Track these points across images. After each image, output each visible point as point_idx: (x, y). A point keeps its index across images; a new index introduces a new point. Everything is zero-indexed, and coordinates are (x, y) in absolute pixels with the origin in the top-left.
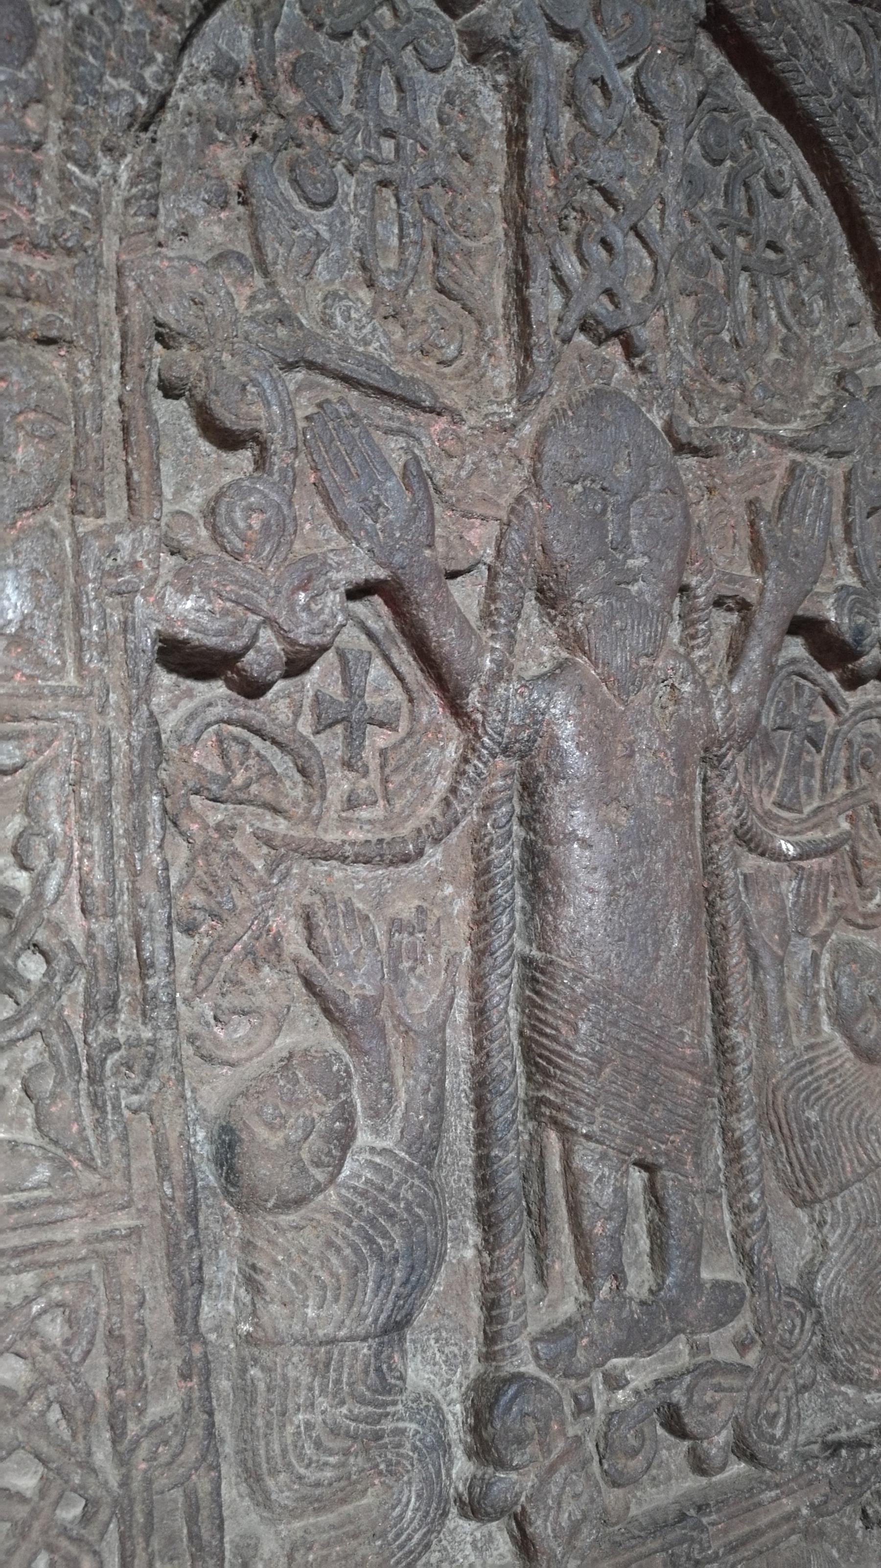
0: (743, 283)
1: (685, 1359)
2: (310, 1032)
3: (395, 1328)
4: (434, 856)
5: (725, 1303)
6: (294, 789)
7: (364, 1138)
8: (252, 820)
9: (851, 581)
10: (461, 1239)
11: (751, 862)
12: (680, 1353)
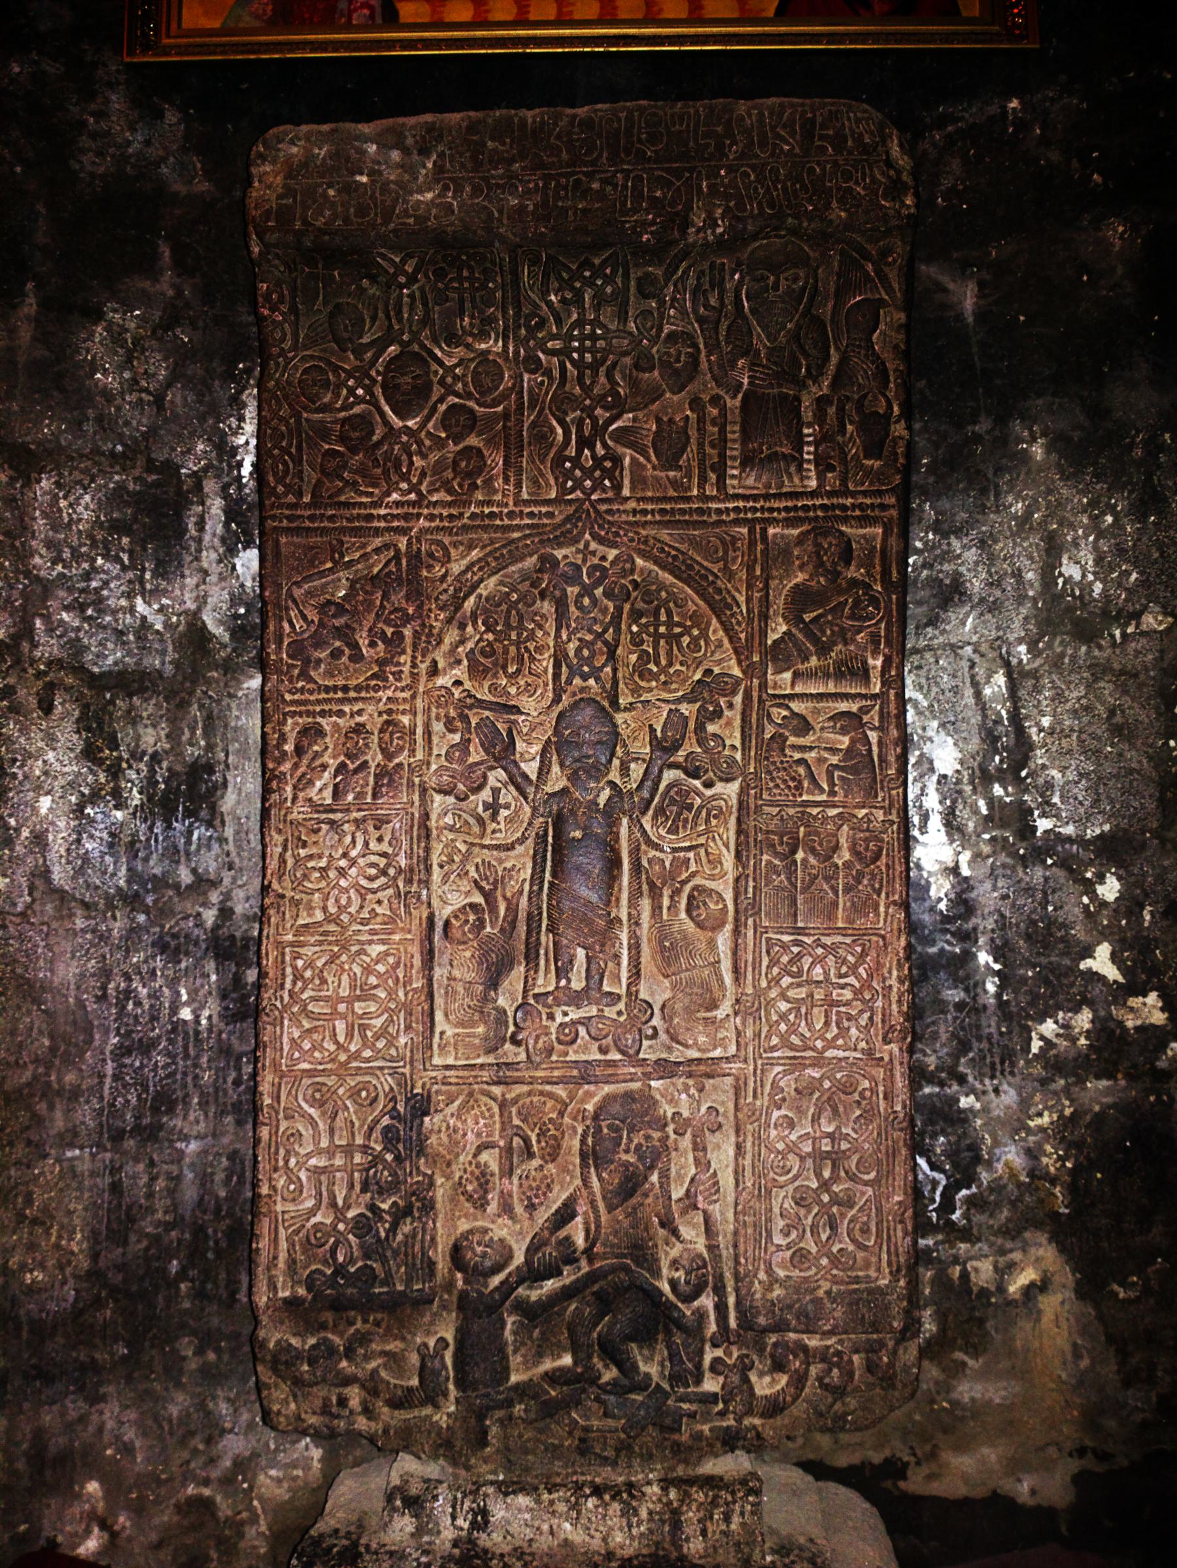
0: (662, 642)
1: (594, 1012)
2: (478, 899)
3: (493, 983)
4: (520, 849)
5: (614, 998)
6: (476, 829)
7: (488, 929)
8: (462, 837)
10: (520, 963)
11: (652, 853)
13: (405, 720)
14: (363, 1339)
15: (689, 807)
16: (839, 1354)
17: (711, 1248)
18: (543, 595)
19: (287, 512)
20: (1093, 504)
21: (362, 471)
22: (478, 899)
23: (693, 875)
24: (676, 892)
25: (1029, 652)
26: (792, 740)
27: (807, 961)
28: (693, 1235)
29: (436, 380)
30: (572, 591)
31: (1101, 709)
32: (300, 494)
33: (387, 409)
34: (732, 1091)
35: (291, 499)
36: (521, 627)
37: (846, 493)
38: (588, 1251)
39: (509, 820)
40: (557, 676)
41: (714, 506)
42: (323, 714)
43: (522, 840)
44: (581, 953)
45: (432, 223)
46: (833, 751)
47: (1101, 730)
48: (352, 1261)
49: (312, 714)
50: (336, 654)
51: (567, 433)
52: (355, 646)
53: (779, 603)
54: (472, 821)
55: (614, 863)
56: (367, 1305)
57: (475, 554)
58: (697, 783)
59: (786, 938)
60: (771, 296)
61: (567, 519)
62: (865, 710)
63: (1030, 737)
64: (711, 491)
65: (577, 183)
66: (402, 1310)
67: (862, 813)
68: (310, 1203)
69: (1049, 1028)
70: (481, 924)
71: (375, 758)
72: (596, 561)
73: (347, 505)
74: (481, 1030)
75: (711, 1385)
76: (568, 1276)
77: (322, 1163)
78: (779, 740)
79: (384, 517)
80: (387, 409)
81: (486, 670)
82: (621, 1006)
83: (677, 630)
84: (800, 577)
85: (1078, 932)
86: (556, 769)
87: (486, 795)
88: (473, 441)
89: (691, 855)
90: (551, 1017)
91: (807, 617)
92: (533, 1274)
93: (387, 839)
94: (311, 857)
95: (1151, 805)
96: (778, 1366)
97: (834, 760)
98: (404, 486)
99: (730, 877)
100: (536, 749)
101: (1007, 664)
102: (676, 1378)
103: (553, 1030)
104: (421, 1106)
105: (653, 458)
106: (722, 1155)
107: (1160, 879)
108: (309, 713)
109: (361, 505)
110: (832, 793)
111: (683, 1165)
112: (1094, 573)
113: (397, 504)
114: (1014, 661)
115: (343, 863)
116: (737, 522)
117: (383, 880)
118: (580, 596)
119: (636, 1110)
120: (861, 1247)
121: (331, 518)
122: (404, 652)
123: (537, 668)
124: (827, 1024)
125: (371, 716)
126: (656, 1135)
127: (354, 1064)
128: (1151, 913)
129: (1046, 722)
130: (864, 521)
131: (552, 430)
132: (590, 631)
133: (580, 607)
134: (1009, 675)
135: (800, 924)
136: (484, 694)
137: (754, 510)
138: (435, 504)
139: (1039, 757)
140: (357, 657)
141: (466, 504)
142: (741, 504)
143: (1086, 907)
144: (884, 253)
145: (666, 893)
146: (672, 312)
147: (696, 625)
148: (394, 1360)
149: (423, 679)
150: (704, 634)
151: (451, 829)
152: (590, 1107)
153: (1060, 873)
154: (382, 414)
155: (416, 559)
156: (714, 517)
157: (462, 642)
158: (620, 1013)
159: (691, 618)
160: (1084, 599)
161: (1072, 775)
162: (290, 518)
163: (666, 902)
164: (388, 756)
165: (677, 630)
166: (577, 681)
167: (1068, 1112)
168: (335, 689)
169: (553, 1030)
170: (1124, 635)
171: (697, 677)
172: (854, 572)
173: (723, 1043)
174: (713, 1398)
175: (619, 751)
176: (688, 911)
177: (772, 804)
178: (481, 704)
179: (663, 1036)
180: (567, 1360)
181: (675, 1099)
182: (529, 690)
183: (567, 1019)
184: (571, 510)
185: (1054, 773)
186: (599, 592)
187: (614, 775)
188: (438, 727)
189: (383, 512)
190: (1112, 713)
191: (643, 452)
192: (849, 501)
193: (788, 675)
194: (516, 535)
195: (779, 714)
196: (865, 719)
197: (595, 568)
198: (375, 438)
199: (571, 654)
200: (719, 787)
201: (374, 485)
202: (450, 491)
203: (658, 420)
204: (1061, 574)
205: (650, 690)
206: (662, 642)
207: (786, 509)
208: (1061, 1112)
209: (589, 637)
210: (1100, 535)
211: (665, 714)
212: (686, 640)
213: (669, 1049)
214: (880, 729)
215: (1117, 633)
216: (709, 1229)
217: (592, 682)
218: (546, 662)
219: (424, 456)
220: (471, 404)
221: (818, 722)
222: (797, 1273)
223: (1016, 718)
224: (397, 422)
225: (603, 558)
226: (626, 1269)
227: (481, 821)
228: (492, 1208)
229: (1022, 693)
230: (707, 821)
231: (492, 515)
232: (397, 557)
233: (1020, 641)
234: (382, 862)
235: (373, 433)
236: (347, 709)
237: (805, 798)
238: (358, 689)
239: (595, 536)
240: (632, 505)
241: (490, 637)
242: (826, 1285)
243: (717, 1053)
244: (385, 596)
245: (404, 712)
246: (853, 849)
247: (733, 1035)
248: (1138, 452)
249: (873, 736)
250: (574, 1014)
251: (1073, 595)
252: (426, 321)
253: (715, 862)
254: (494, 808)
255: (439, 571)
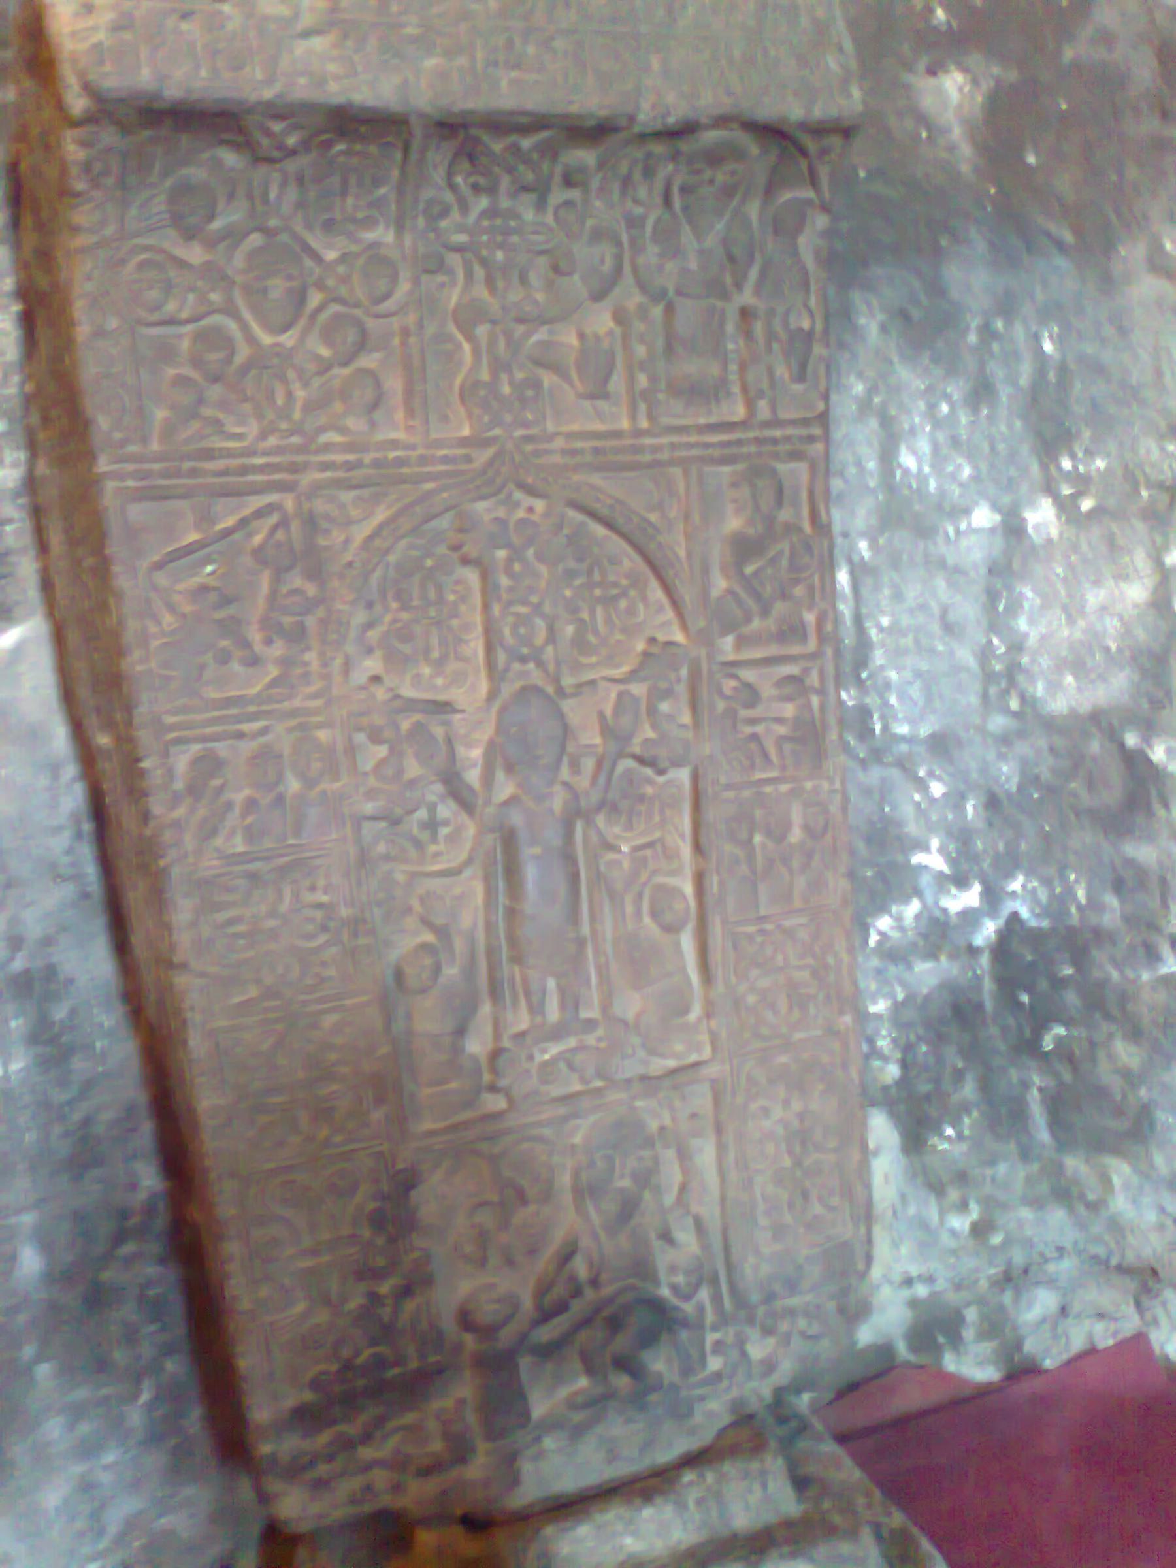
3: (460, 1032)
4: (467, 873)
5: (591, 1024)
6: (413, 853)
9: (651, 734)
11: (611, 856)
12: (572, 1042)
13: (323, 735)
14: (381, 1420)
15: (642, 798)
16: (818, 1307)
17: (705, 1247)
18: (466, 561)
19: (130, 467)
20: (930, 389)
21: (223, 405)
22: (428, 937)
23: (655, 872)
24: (640, 896)
25: (871, 547)
26: (744, 713)
27: (769, 951)
28: (686, 1237)
29: (311, 280)
30: (501, 554)
31: (936, 609)
32: (144, 440)
33: (247, 315)
34: (709, 1096)
35: (132, 448)
36: (441, 600)
37: (775, 423)
38: (594, 1282)
39: (452, 839)
40: (490, 664)
41: (648, 441)
42: (216, 738)
43: (470, 861)
44: (551, 984)
45: (333, 87)
46: (779, 720)
47: (936, 627)
48: (357, 1354)
49: (204, 739)
50: (224, 659)
51: (476, 352)
52: (246, 644)
53: (717, 553)
54: (408, 846)
55: (575, 877)
56: (378, 1390)
57: (381, 515)
58: (649, 771)
59: (751, 929)
60: (706, 191)
61: (490, 463)
62: (806, 671)
63: (869, 637)
64: (644, 424)
65: (510, 44)
66: (418, 1385)
67: (808, 785)
68: (300, 1307)
69: (884, 923)
70: (437, 969)
71: (293, 785)
72: (521, 514)
73: (209, 454)
74: (454, 1085)
75: (714, 1364)
76: (577, 1308)
77: (308, 1263)
78: (731, 714)
79: (262, 469)
80: (247, 315)
81: (406, 659)
82: (600, 1032)
83: (615, 591)
84: (733, 523)
85: (912, 828)
86: (500, 775)
87: (422, 814)
88: (368, 361)
89: (648, 852)
90: (531, 1058)
91: (749, 570)
92: (545, 1316)
93: (321, 883)
94: (231, 922)
95: (974, 700)
96: (768, 1332)
97: (782, 730)
98: (284, 426)
99: (688, 871)
100: (476, 753)
101: (850, 561)
102: (687, 1371)
103: (534, 1071)
104: (407, 1182)
105: (577, 383)
106: (706, 1155)
107: (984, 770)
108: (204, 739)
109: (230, 454)
110: (783, 768)
111: (672, 1174)
112: (932, 466)
113: (279, 450)
114: (856, 559)
115: (271, 923)
116: (671, 462)
117: (323, 938)
118: (509, 561)
119: (627, 1133)
120: (831, 1209)
121: (193, 473)
122: (308, 648)
123: (466, 651)
124: (791, 1008)
125: (281, 736)
126: (646, 1153)
127: (326, 1152)
128: (975, 807)
129: (885, 621)
130: (796, 456)
131: (459, 346)
132: (525, 602)
133: (509, 572)
134: (852, 573)
135: (763, 912)
136: (408, 692)
137: (691, 446)
138: (328, 447)
139: (879, 657)
140: (254, 661)
141: (365, 449)
142: (675, 439)
143: (918, 804)
144: (824, 152)
145: (629, 899)
146: (597, 203)
147: (634, 585)
148: (415, 1430)
149: (337, 678)
150: (644, 599)
151: (387, 858)
152: (577, 1139)
153: (895, 773)
154: (244, 327)
155: (311, 523)
156: (647, 457)
157: (370, 625)
158: (599, 1040)
159: (627, 576)
160: (921, 493)
161: (908, 674)
162: (136, 475)
163: (629, 909)
164: (309, 783)
165: (615, 591)
166: (517, 666)
167: (900, 997)
168: (228, 702)
169: (534, 1071)
170: (958, 532)
171: (640, 646)
172: (785, 515)
173: (699, 1048)
174: (718, 1376)
175: (570, 748)
176: (654, 915)
177: (728, 787)
178: (411, 705)
179: (641, 1054)
180: (583, 1382)
181: (654, 1114)
182: (458, 679)
183: (547, 1057)
184: (490, 452)
185: (893, 675)
186: (530, 552)
187: (565, 773)
188: (360, 738)
189: (259, 461)
190: (945, 611)
191: (566, 377)
192: (778, 433)
193: (730, 639)
194: (429, 486)
195: (729, 685)
196: (808, 682)
197: (521, 522)
198: (239, 359)
199: (507, 631)
200: (673, 774)
201: (242, 423)
202: (343, 431)
203: (581, 336)
204: (900, 466)
205: (592, 666)
206: (599, 611)
207: (724, 445)
208: (894, 997)
209: (524, 610)
210: (937, 424)
211: (613, 695)
212: (623, 604)
213: (646, 1063)
214: (821, 692)
215: (951, 530)
216: (700, 1228)
217: (531, 666)
218: (476, 646)
219: (306, 385)
220: (357, 312)
221: (768, 691)
222: (778, 1247)
223: (858, 620)
224: (267, 339)
225: (530, 510)
226: (633, 1288)
227: (419, 845)
228: (494, 1260)
229: (864, 591)
230: (662, 812)
231: (400, 462)
232: (284, 523)
233: (863, 534)
234: (319, 915)
235: (233, 353)
236: (245, 727)
237: (759, 775)
238: (258, 699)
239: (522, 486)
240: (559, 443)
241: (405, 616)
242: (805, 1252)
243: (694, 1058)
244: (277, 580)
245: (320, 726)
246: (807, 828)
247: (705, 1038)
248: (972, 338)
249: (815, 700)
250: (554, 1050)
251: (910, 487)
252: (301, 205)
253: (671, 855)
254: (432, 825)
255: (337, 536)
